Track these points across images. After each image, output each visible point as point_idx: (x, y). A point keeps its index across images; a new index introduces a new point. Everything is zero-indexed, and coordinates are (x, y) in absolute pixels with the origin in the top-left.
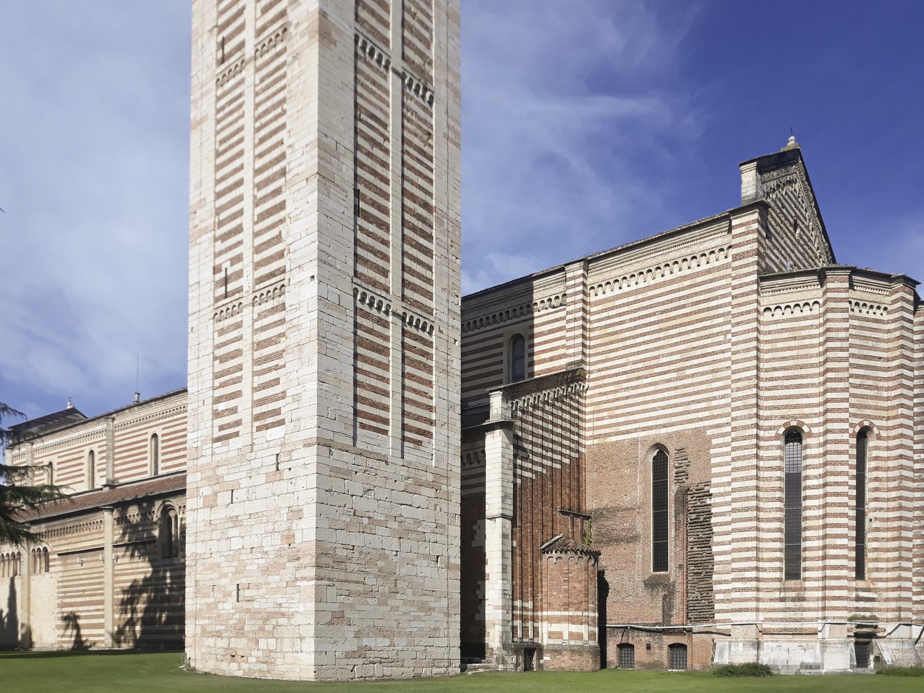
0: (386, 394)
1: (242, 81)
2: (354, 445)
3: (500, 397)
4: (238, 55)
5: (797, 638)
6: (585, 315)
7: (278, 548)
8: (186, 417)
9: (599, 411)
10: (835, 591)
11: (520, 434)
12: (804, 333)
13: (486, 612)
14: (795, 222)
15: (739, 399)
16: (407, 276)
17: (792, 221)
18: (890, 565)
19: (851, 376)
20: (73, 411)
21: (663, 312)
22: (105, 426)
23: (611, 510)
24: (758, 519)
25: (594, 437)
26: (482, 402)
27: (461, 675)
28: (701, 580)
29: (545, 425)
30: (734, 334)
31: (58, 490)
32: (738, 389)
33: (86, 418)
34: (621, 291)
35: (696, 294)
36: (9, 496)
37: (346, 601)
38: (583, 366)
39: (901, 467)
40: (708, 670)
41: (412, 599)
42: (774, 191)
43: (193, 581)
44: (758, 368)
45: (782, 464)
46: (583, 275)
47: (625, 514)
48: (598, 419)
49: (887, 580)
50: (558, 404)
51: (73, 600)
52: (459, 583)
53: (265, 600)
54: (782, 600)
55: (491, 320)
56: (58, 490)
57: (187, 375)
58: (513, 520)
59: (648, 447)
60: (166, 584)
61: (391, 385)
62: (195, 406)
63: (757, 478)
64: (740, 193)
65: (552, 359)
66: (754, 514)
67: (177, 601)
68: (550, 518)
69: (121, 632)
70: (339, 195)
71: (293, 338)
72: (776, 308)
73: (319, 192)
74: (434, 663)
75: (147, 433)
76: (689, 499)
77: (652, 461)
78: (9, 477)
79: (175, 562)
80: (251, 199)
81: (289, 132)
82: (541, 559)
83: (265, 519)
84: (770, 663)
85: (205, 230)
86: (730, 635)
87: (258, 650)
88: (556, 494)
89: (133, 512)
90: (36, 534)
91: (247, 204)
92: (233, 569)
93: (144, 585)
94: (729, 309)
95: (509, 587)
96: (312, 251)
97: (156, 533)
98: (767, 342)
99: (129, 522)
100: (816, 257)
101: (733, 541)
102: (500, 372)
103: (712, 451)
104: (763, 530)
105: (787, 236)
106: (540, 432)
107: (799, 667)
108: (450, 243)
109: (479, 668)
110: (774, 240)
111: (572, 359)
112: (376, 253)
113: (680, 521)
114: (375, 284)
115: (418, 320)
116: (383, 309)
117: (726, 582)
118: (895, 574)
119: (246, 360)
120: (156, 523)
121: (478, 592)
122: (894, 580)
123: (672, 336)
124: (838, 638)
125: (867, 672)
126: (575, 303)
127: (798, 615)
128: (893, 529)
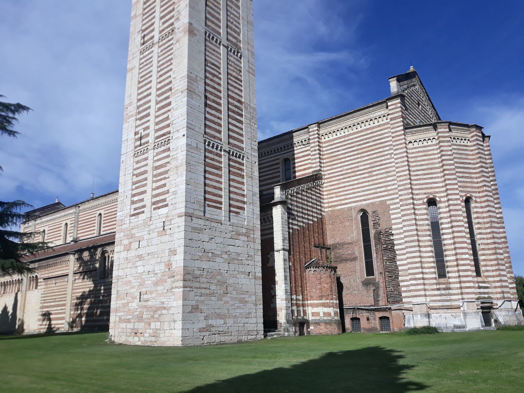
0: (221, 189)
1: (152, 52)
2: (204, 216)
3: (279, 189)
4: (151, 41)
5: (450, 311)
6: (320, 148)
7: (163, 271)
8: (117, 204)
9: (330, 194)
10: (466, 284)
11: (290, 207)
12: (430, 153)
13: (277, 302)
14: (418, 102)
16: (231, 133)
17: (417, 102)
18: (494, 268)
19: (457, 172)
20: (59, 203)
21: (358, 145)
22: (74, 210)
24: (419, 246)
25: (329, 207)
26: (270, 191)
27: (264, 339)
28: (393, 280)
29: (303, 202)
30: (395, 155)
31: (47, 244)
32: (401, 181)
33: (65, 207)
34: (336, 137)
35: (374, 136)
36: (20, 249)
37: (199, 299)
38: (321, 172)
39: (490, 216)
40: (403, 331)
41: (236, 297)
42: (406, 89)
43: (116, 291)
44: (409, 170)
45: (429, 217)
46: (318, 130)
47: (348, 246)
48: (330, 198)
49: (493, 276)
50: (309, 191)
51: (49, 304)
52: (261, 287)
53: (155, 300)
54: (438, 289)
55: (273, 152)
56: (47, 244)
57: (118, 183)
58: (289, 251)
59: (357, 211)
60: (101, 293)
61: (223, 185)
62: (122, 199)
63: (416, 225)
64: (390, 91)
65: (304, 169)
66: (417, 243)
67: (106, 303)
68: (308, 250)
69: (74, 321)
70: (197, 98)
71: (173, 164)
72: (414, 142)
73: (188, 97)
74: (249, 333)
75: (96, 213)
76: (382, 237)
78: (21, 238)
79: (107, 281)
80: (155, 101)
81: (174, 72)
82: (305, 272)
83: (156, 256)
84: (437, 326)
85: (132, 116)
86: (412, 311)
87: (150, 329)
89: (86, 255)
90: (33, 268)
91: (153, 104)
92: (138, 284)
93: (88, 294)
94: (391, 143)
95: (289, 288)
96: (184, 123)
97: (97, 265)
98: (412, 157)
99: (83, 260)
100: (431, 118)
101: (408, 258)
102: (279, 176)
103: (391, 212)
104: (423, 252)
105: (415, 109)
106: (301, 205)
107: (453, 328)
108: (251, 117)
109: (274, 335)
110: (409, 111)
111: (315, 169)
112: (215, 123)
113: (378, 249)
114: (215, 137)
115: (237, 153)
116: (219, 149)
117: (407, 281)
118: (497, 273)
119: (149, 176)
120: (98, 260)
121: (272, 291)
122: (497, 276)
123: (364, 157)
124: (472, 310)
125: (492, 329)
126: (314, 142)
127: (448, 298)
128: (492, 249)
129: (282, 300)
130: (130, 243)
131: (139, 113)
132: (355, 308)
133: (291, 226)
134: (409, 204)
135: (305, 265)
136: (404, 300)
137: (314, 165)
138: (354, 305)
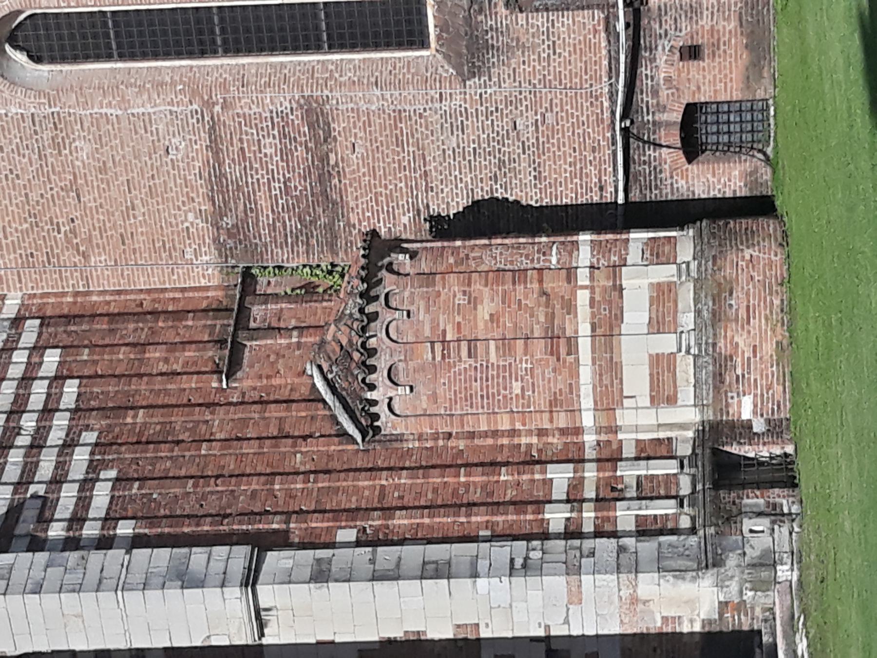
23: (219, 199)
68: (254, 413)
77: (45, 68)
82: (400, 438)
88: (167, 392)
129: (575, 597)
132: (625, 131)
133: (91, 530)
135: (354, 442)
138: (602, 136)
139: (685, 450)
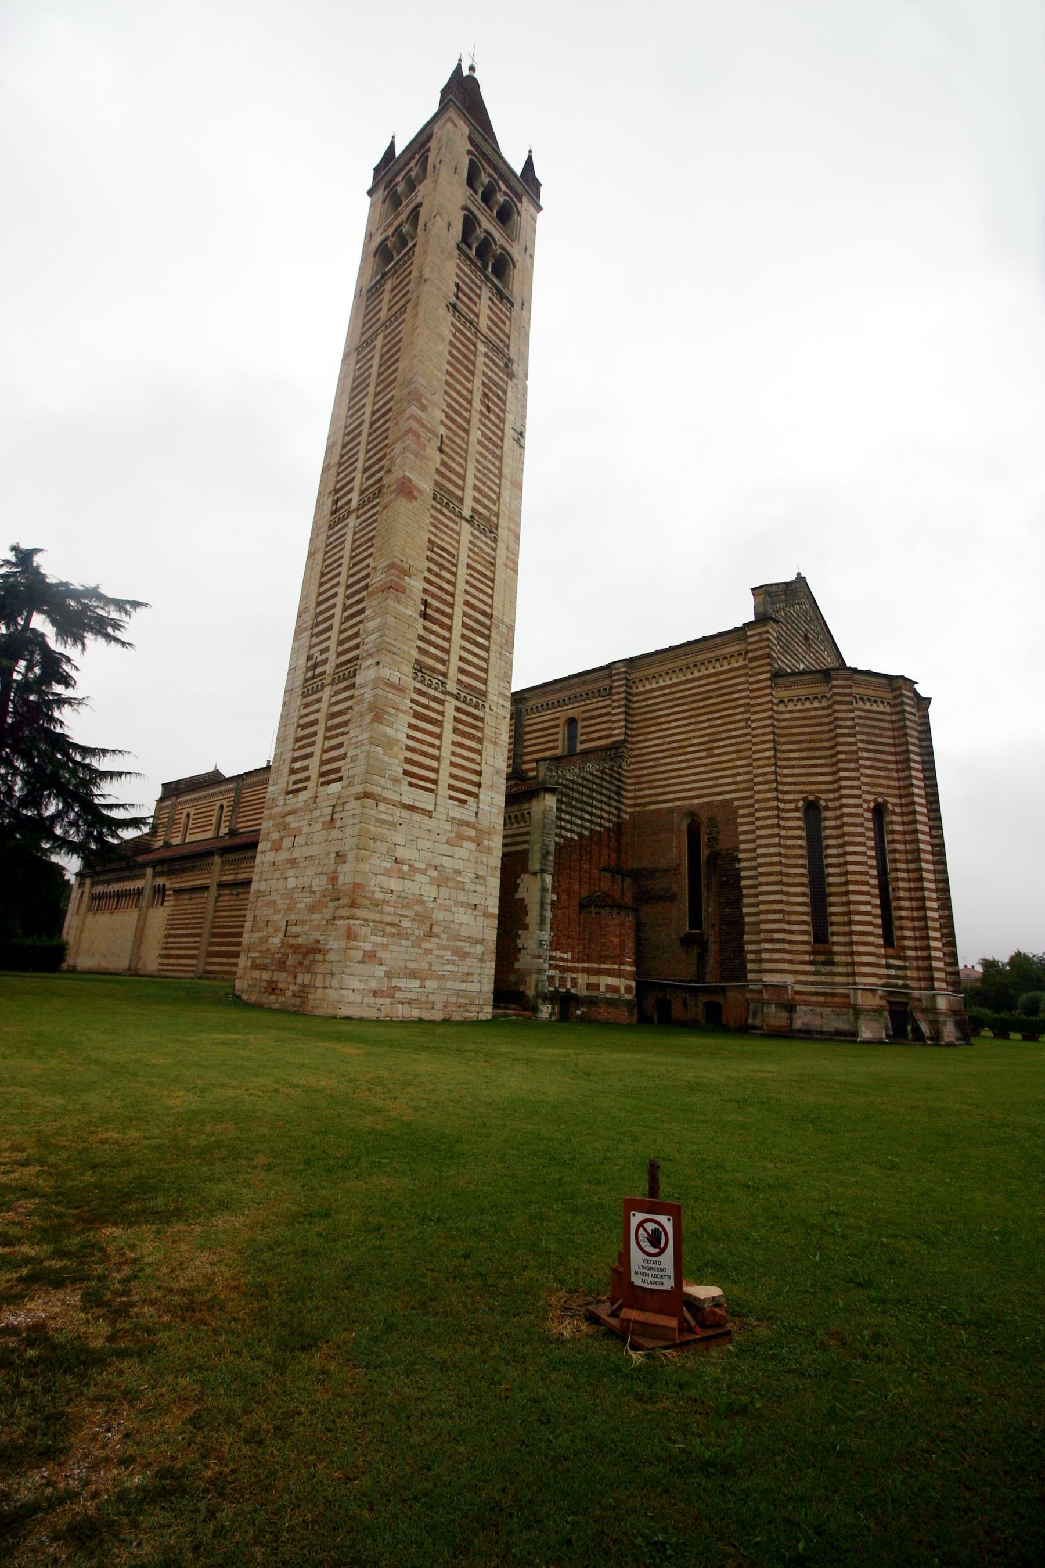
9: (640, 783)
15: (760, 775)
21: (692, 702)
32: (759, 767)
46: (626, 672)
103: (739, 820)
111: (617, 739)
130: (282, 839)
131: (317, 624)
134: (771, 809)
136: (750, 976)
137: (616, 732)
139: (573, 991)
